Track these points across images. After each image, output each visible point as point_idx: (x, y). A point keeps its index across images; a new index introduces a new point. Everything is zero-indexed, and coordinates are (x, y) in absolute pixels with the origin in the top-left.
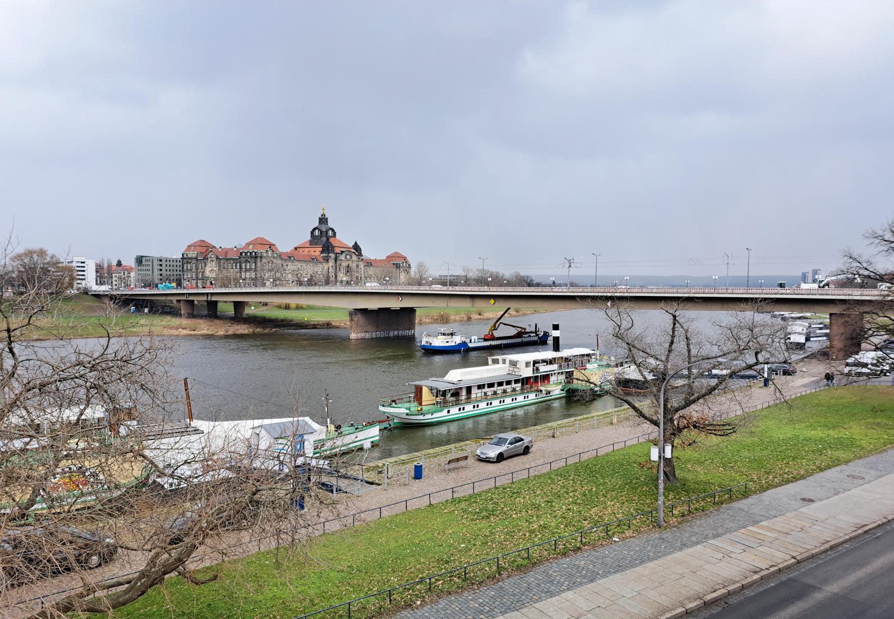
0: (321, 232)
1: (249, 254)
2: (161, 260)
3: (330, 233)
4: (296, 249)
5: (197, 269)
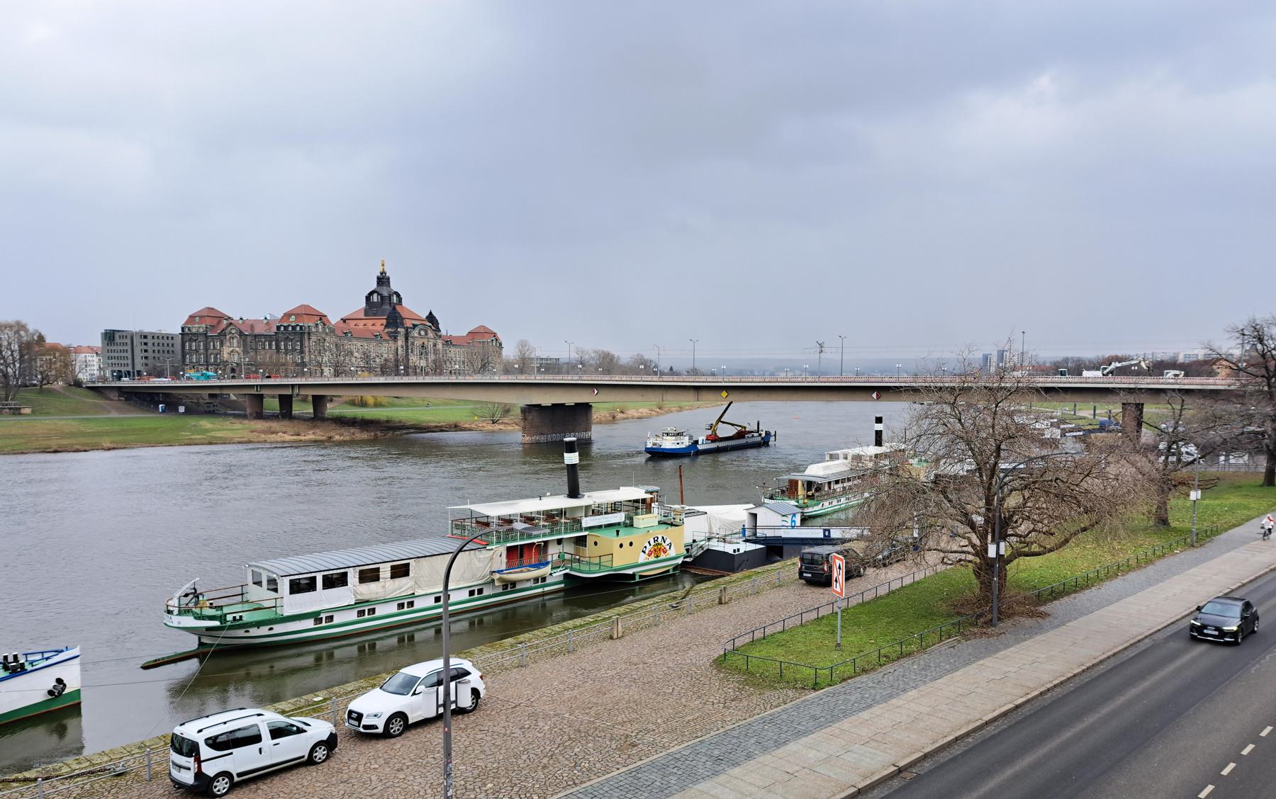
0: (382, 297)
2: (145, 337)
3: (395, 298)
4: (344, 320)
5: (206, 349)
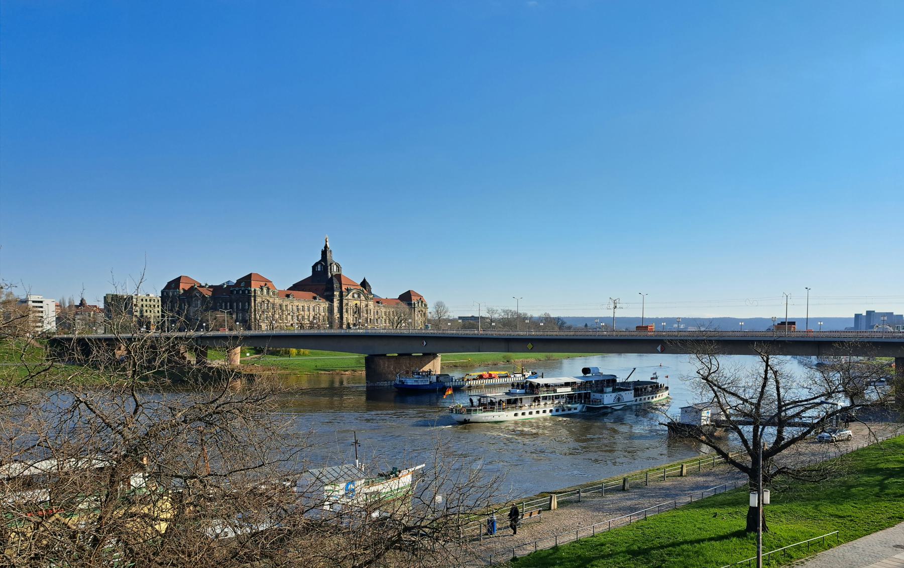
1: (241, 292)
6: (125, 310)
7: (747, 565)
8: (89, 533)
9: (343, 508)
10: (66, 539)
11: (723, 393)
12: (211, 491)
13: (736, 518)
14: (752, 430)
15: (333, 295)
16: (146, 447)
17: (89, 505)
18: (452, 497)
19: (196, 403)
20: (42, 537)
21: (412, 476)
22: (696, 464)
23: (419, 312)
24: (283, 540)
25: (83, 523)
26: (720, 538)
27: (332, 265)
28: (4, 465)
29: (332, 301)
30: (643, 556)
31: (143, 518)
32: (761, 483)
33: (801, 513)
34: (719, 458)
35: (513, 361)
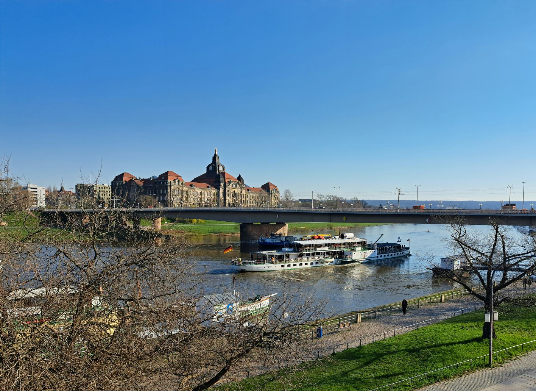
1: (162, 183)
6: (89, 194)
7: (483, 359)
8: (66, 334)
9: (226, 320)
10: (51, 338)
11: (469, 250)
12: (142, 309)
13: (476, 329)
14: (486, 273)
15: (220, 185)
16: (101, 281)
17: (66, 317)
18: (294, 314)
19: (133, 253)
20: (36, 337)
21: (269, 300)
22: (451, 295)
23: (274, 196)
24: (187, 340)
25: (62, 328)
26: (466, 342)
27: (219, 166)
28: (13, 291)
29: (219, 189)
30: (416, 353)
31: (99, 326)
32: (492, 307)
33: (518, 327)
34: (465, 291)
35: (334, 228)
